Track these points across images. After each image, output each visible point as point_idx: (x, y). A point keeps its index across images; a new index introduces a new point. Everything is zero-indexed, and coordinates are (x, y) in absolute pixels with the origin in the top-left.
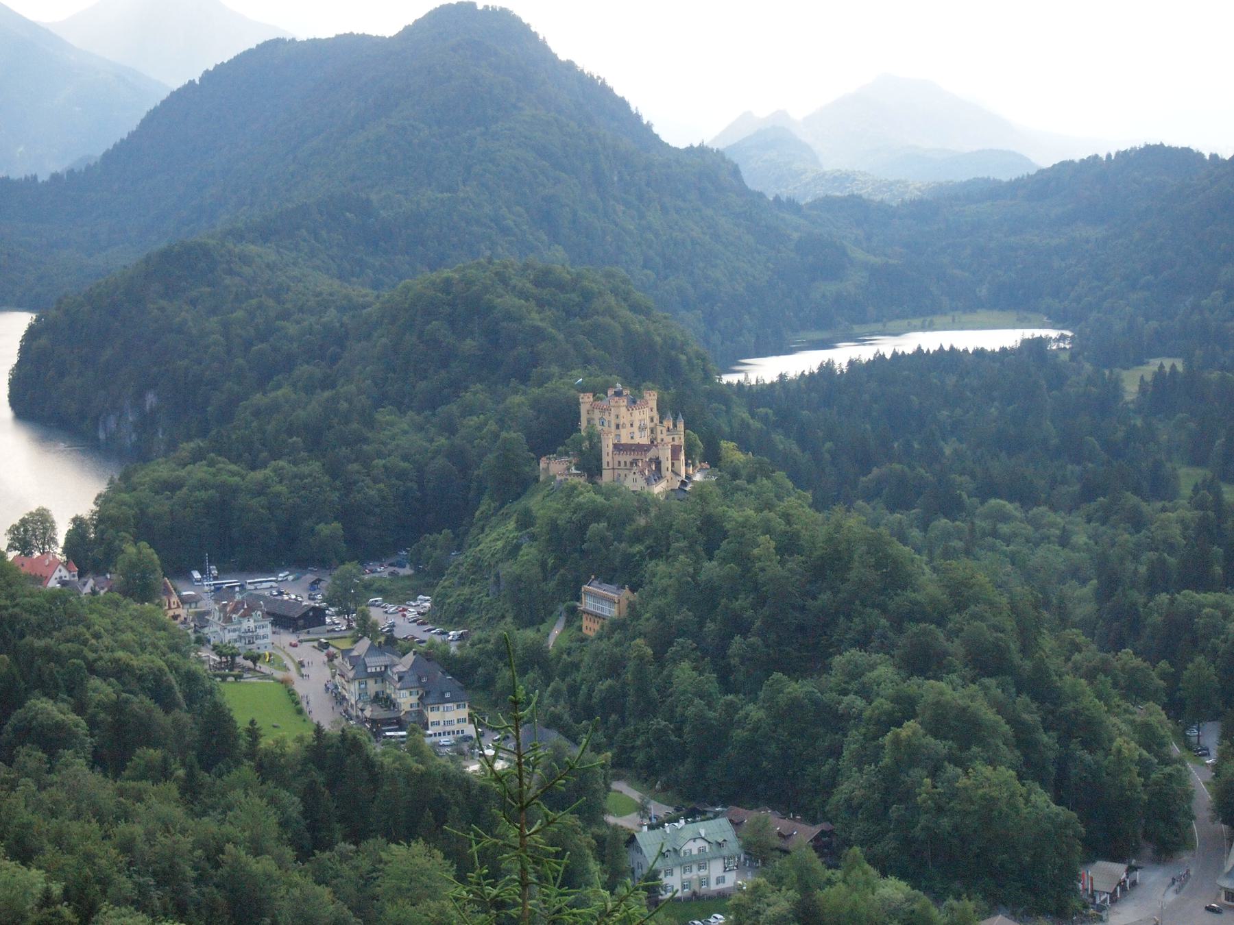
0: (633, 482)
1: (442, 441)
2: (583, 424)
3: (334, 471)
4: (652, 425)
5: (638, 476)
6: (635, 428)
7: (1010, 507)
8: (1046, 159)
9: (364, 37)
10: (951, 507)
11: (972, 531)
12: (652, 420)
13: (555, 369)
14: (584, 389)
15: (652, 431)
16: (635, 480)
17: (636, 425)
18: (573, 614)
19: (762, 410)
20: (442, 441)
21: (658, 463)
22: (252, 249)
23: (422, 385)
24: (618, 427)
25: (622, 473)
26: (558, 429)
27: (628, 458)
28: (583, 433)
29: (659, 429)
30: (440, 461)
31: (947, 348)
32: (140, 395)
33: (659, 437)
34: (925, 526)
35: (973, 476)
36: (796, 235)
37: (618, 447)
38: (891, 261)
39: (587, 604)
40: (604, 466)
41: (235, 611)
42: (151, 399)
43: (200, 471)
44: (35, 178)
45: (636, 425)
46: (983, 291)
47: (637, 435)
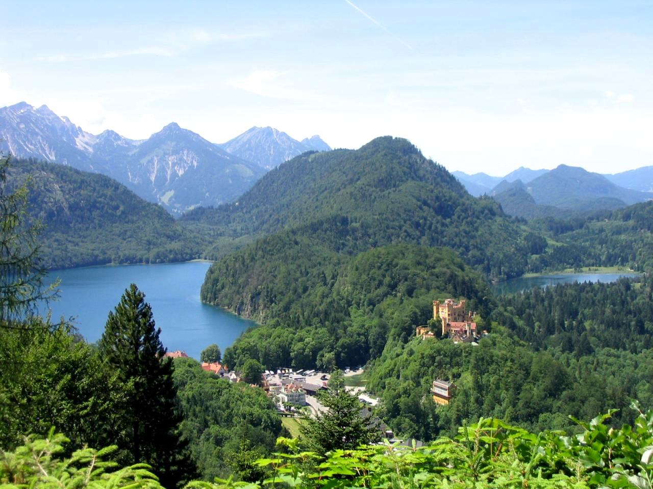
3: (332, 331)
7: (613, 351)
8: (630, 202)
9: (346, 150)
10: (590, 351)
11: (598, 360)
13: (423, 290)
19: (509, 308)
21: (466, 332)
23: (368, 295)
24: (449, 315)
26: (424, 317)
28: (435, 319)
30: (377, 329)
31: (588, 282)
34: (578, 357)
35: (599, 338)
36: (525, 234)
38: (565, 245)
43: (278, 331)
44: (212, 208)
46: (603, 258)
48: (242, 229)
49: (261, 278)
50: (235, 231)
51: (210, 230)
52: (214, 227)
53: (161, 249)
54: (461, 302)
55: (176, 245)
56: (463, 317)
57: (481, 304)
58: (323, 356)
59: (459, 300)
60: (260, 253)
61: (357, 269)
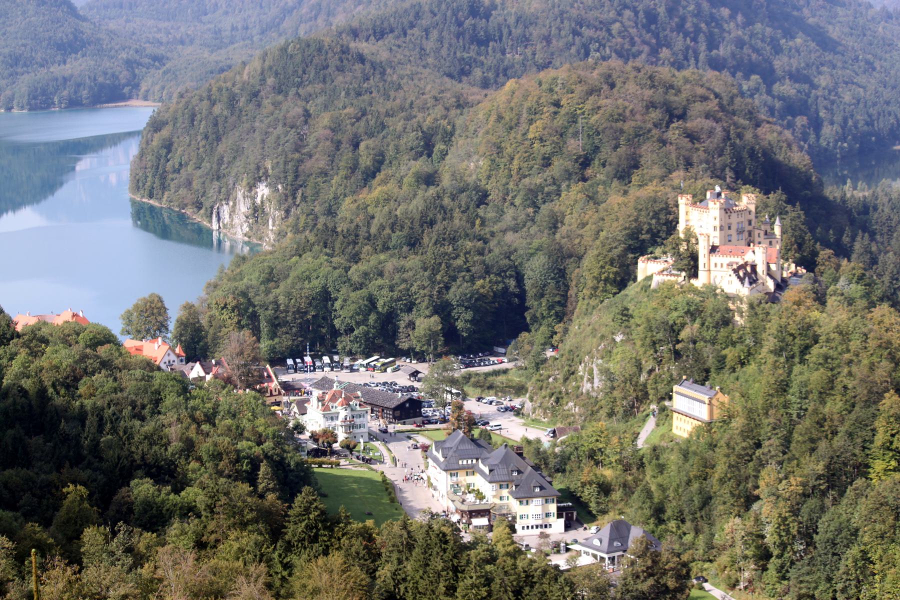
0: (732, 285)
1: (544, 239)
2: (681, 227)
4: (750, 228)
5: (734, 278)
6: (733, 232)
12: (750, 223)
13: (657, 171)
14: (682, 192)
15: (750, 234)
16: (730, 282)
17: (734, 227)
18: (665, 414)
20: (544, 239)
22: (364, 47)
25: (719, 274)
26: (655, 231)
27: (726, 260)
29: (757, 232)
32: (251, 187)
33: (757, 240)
37: (713, 249)
39: (678, 402)
40: (701, 266)
41: (334, 399)
42: (263, 191)
45: (734, 227)
47: (734, 237)
48: (234, 28)
49: (271, 140)
50: (218, 32)
51: (159, 30)
52: (166, 24)
53: (42, 74)
54: (748, 200)
55: (76, 66)
56: (750, 234)
57: (794, 206)
58: (412, 325)
59: (739, 193)
60: (270, 81)
61: (500, 118)
